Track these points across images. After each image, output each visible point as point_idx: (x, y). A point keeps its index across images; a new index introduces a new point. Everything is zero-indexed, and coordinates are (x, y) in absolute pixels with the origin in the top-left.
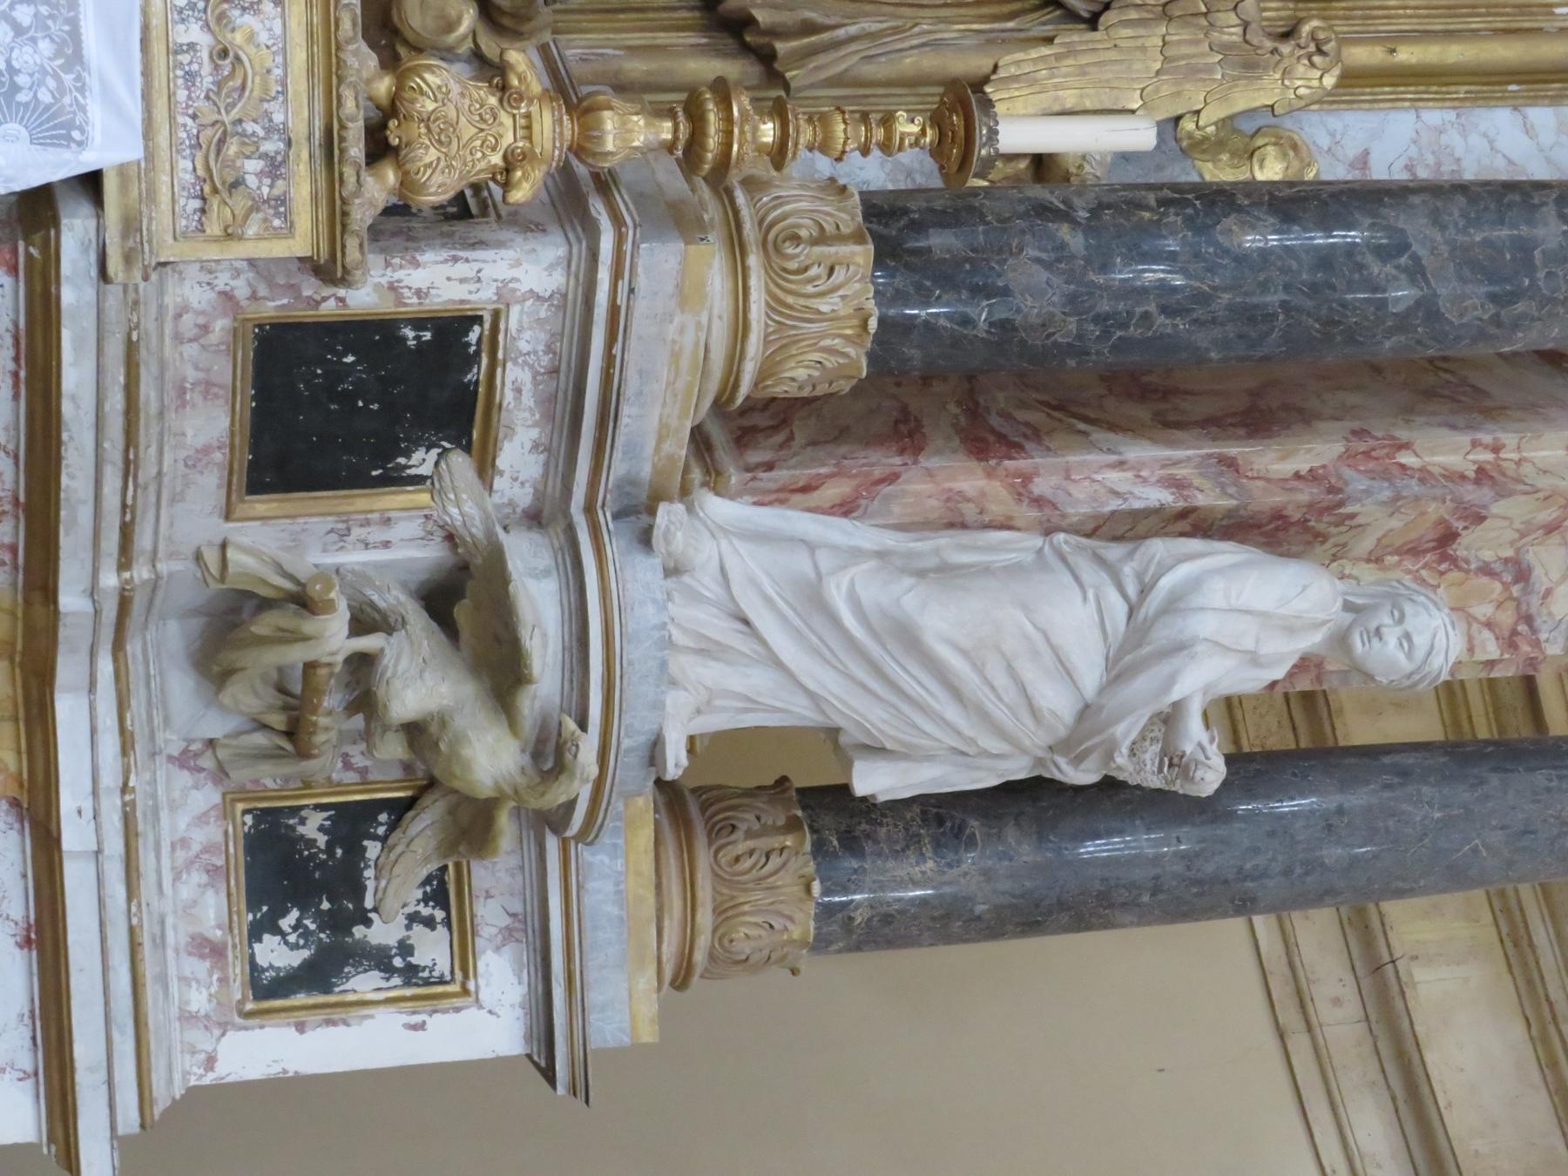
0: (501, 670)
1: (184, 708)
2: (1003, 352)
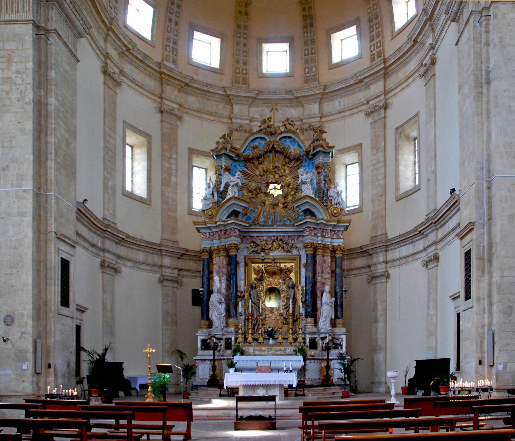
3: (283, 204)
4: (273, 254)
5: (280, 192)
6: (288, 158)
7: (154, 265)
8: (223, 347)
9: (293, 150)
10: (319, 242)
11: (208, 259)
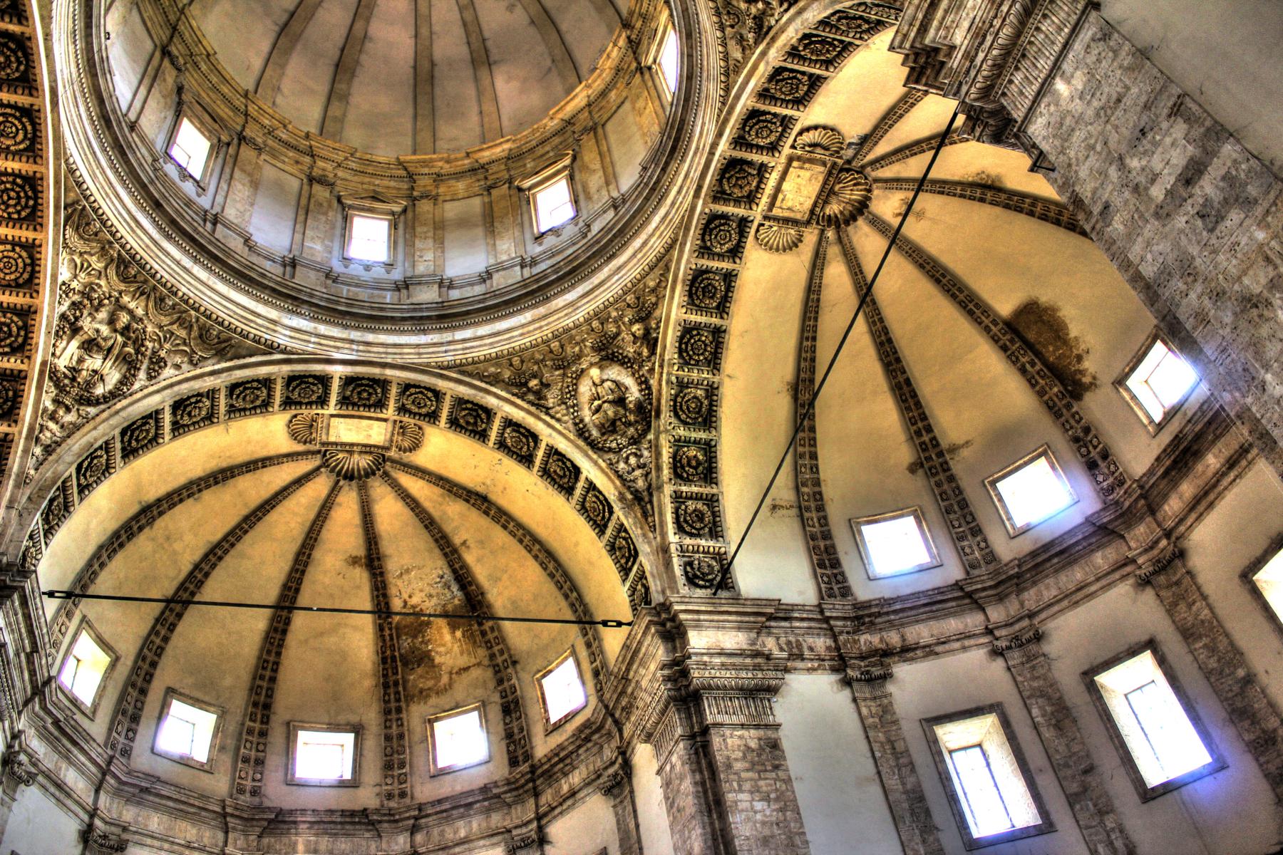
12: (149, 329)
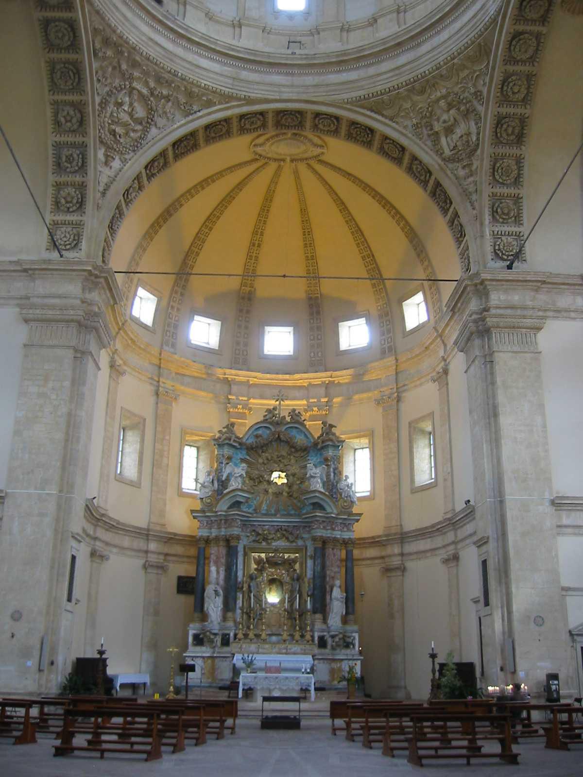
0: (336, 635)
1: (338, 651)
2: (322, 608)
3: (288, 493)
4: (275, 544)
5: (285, 481)
6: (294, 447)
7: (139, 551)
8: (219, 643)
9: (299, 439)
10: (329, 535)
11: (204, 548)
12: (456, 89)
